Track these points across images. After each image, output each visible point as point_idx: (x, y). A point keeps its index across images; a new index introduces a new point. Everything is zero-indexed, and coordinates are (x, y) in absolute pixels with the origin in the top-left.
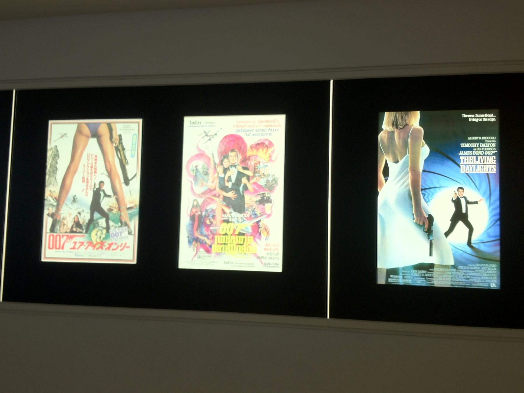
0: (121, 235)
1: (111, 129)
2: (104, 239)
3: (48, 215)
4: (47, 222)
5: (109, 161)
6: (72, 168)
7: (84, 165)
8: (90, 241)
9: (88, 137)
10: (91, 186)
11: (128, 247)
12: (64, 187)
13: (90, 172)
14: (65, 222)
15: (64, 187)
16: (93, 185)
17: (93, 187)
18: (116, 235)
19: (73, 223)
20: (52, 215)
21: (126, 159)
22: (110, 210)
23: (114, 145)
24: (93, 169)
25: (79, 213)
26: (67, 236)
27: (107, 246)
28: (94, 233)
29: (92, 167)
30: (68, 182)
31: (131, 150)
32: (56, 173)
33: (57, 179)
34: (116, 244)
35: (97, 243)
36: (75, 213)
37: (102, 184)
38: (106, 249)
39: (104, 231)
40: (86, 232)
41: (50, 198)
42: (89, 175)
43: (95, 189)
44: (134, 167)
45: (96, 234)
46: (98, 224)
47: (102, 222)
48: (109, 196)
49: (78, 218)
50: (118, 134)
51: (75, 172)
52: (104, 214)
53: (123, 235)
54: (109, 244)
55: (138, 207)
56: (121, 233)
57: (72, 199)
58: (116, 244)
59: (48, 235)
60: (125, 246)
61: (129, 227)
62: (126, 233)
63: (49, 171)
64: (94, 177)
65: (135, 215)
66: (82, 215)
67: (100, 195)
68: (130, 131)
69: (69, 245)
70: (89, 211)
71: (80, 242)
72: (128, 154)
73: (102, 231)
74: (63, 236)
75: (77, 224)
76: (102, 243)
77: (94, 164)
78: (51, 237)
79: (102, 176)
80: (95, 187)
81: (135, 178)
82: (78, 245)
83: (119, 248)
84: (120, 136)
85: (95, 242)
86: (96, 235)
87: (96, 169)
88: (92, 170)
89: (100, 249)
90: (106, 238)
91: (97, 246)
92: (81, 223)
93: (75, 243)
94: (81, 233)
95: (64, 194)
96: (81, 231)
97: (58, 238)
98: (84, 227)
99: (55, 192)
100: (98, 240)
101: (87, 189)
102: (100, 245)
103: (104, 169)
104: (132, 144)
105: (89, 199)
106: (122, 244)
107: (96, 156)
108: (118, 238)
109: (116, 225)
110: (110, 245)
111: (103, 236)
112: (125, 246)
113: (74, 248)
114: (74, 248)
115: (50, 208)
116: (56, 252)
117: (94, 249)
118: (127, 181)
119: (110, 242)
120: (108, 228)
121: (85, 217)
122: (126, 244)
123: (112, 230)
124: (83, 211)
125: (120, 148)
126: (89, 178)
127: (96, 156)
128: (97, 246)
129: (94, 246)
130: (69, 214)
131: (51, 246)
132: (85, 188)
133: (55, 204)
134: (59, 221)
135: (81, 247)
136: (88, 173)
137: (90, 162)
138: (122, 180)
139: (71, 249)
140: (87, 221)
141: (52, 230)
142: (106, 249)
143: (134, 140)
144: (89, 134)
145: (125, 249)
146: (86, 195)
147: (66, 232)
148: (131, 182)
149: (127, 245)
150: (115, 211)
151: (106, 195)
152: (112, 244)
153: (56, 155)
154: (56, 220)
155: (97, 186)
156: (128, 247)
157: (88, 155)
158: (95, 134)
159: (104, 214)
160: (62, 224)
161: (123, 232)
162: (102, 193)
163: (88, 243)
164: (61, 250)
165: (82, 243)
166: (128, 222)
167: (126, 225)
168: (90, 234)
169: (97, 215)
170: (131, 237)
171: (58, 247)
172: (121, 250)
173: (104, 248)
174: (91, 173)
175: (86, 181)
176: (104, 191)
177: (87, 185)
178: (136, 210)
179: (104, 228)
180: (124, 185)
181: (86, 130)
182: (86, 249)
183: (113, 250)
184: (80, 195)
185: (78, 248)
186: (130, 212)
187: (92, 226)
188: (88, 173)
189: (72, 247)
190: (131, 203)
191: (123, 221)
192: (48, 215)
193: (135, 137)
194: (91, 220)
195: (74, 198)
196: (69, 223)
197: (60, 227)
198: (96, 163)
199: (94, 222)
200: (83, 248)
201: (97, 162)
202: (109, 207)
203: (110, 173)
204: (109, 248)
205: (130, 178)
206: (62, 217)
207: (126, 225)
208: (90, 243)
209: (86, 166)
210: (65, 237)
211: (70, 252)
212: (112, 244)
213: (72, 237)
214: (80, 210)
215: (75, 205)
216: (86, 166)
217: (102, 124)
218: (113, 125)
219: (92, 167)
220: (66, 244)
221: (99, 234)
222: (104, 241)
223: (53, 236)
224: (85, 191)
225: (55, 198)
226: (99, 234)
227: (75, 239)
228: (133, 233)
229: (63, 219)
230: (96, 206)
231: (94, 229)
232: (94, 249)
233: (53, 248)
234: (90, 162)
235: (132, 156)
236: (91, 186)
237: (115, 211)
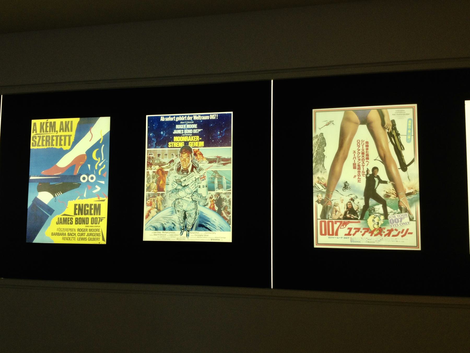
0: (401, 221)
1: (382, 116)
2: (382, 225)
3: (318, 201)
4: (318, 209)
5: (382, 147)
6: (341, 155)
7: (355, 152)
8: (367, 227)
9: (357, 124)
10: (363, 172)
11: (411, 233)
12: (334, 173)
13: (361, 158)
14: (337, 208)
15: (334, 173)
16: (365, 170)
17: (366, 173)
18: (396, 221)
19: (346, 210)
20: (322, 202)
21: (401, 144)
22: (387, 196)
23: (387, 131)
24: (365, 155)
25: (352, 200)
26: (341, 222)
27: (386, 232)
28: (370, 219)
29: (363, 153)
30: (337, 168)
31: (407, 135)
32: (324, 161)
33: (325, 165)
34: (396, 230)
35: (375, 229)
36: (347, 200)
37: (376, 170)
38: (385, 235)
39: (382, 218)
40: (362, 218)
41: (319, 185)
42: (361, 161)
43: (368, 176)
44: (411, 152)
45: (373, 221)
46: (374, 210)
47: (379, 208)
48: (385, 182)
49: (352, 204)
50: (391, 119)
51: (345, 158)
52: (379, 200)
53: (403, 221)
54: (388, 230)
55: (418, 193)
56: (401, 219)
57: (343, 186)
58: (396, 230)
59: (319, 221)
60: (407, 232)
61: (409, 213)
62: (407, 219)
63: (315, 158)
64: (366, 163)
65: (416, 201)
66: (356, 201)
67: (375, 181)
68: (404, 117)
69: (343, 231)
70: (364, 198)
71: (355, 229)
72: (403, 140)
73: (379, 218)
74: (336, 223)
75: (351, 210)
76: (380, 231)
77: (365, 150)
78: (323, 223)
79: (374, 161)
80: (368, 174)
81: (413, 163)
82: (353, 231)
83: (401, 234)
84: (393, 122)
85: (372, 229)
86: (371, 222)
87: (367, 155)
88: (363, 156)
89: (379, 236)
90: (384, 224)
91: (375, 233)
92: (355, 210)
93: (350, 229)
94: (357, 219)
95: (334, 181)
96: (356, 217)
97: (330, 223)
98: (358, 214)
99: (323, 178)
100: (376, 226)
101: (359, 175)
102: (378, 231)
103: (377, 155)
104: (408, 129)
105: (362, 185)
106: (403, 230)
107: (367, 142)
108: (399, 224)
109: (395, 211)
110: (390, 231)
111: (381, 222)
112: (407, 232)
113: (349, 234)
114: (349, 234)
115: (320, 195)
116: (329, 238)
117: (371, 235)
118: (404, 167)
119: (390, 229)
120: (386, 214)
121: (360, 203)
122: (408, 230)
123: (390, 216)
124: (357, 197)
125: (394, 133)
126: (361, 164)
127: (367, 142)
128: (375, 233)
129: (372, 233)
130: (340, 200)
131: (323, 233)
132: (356, 174)
133: (325, 190)
134: (330, 208)
135: (357, 233)
136: (359, 160)
137: (361, 148)
138: (399, 166)
139: (346, 235)
140: (362, 208)
141: (324, 215)
142: (385, 235)
143: (409, 125)
144: (358, 121)
145: (407, 235)
146: (359, 181)
147: (339, 219)
148: (408, 167)
149: (409, 231)
150: (392, 197)
151: (381, 181)
152: (392, 230)
153: (323, 143)
154: (327, 207)
155: (371, 172)
156: (411, 233)
157: (358, 142)
158: (365, 121)
159: (379, 200)
160: (334, 211)
161: (404, 218)
162: (376, 179)
163: (364, 229)
164: (334, 236)
165: (358, 230)
166: (408, 208)
167: (406, 211)
168: (366, 220)
169: (372, 202)
170: (413, 224)
171: (331, 233)
172: (402, 236)
173: (383, 234)
174: (363, 160)
175: (357, 167)
176: (378, 177)
177: (359, 172)
178: (417, 196)
179: (381, 214)
180: (400, 171)
181: (355, 117)
182: (363, 235)
183: (393, 236)
184: (352, 181)
185: (354, 235)
186: (409, 197)
187: (367, 213)
188: (359, 160)
189: (347, 233)
190: (410, 188)
191: (402, 207)
192: (318, 201)
193: (410, 121)
194: (366, 206)
195: (345, 185)
196: (342, 209)
197: (332, 214)
198: (367, 149)
199: (370, 208)
200: (359, 234)
201: (369, 148)
202: (385, 193)
203: (384, 159)
204: (389, 234)
205: (407, 163)
206: (333, 203)
207: (406, 211)
208: (367, 230)
209: (356, 152)
210: (338, 224)
211: (345, 238)
212: (392, 230)
213: (346, 224)
214: (353, 196)
215: (347, 192)
216: (356, 152)
217: (373, 111)
218: (384, 111)
219: (363, 153)
220: (340, 230)
221: (376, 220)
222: (382, 227)
223: (325, 222)
224: (357, 177)
225: (325, 185)
226: (376, 220)
227: (349, 226)
228: (415, 219)
229: (334, 206)
230: (370, 192)
231: (370, 215)
232: (371, 235)
233: (325, 234)
234: (361, 148)
235: (408, 141)
236: (363, 172)
237: (392, 197)
